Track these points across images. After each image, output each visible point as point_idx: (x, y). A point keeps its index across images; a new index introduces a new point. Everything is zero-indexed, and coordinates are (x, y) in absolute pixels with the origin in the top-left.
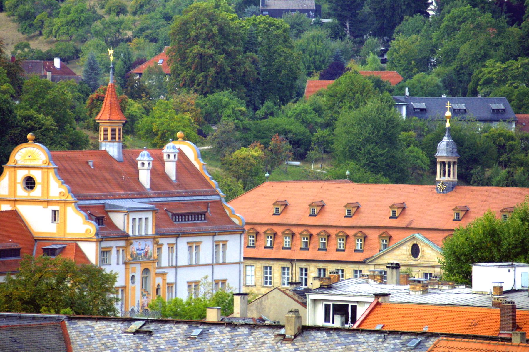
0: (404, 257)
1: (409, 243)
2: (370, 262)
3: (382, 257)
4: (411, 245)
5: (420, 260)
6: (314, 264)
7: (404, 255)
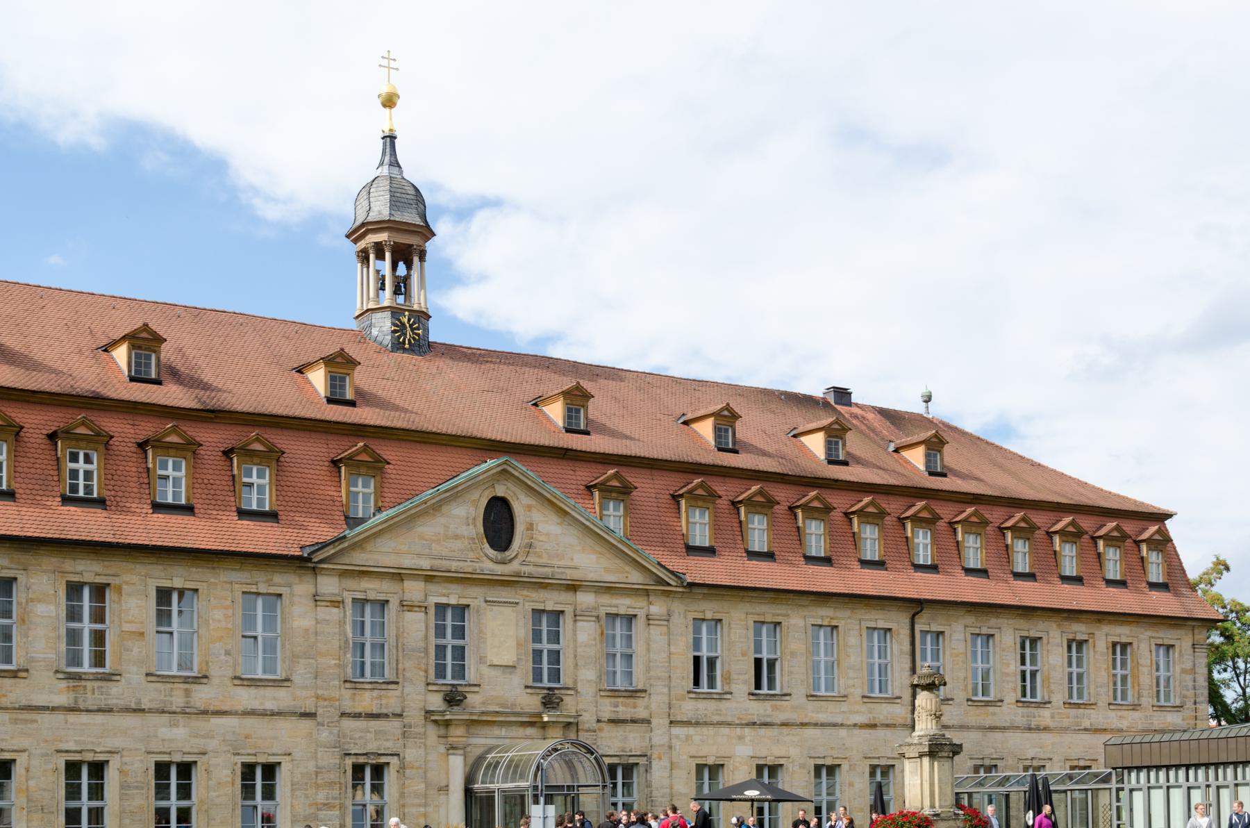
0: (458, 545)
1: (475, 495)
2: (321, 561)
3: (369, 547)
4: (484, 502)
5: (517, 562)
6: (50, 561)
7: (457, 537)
